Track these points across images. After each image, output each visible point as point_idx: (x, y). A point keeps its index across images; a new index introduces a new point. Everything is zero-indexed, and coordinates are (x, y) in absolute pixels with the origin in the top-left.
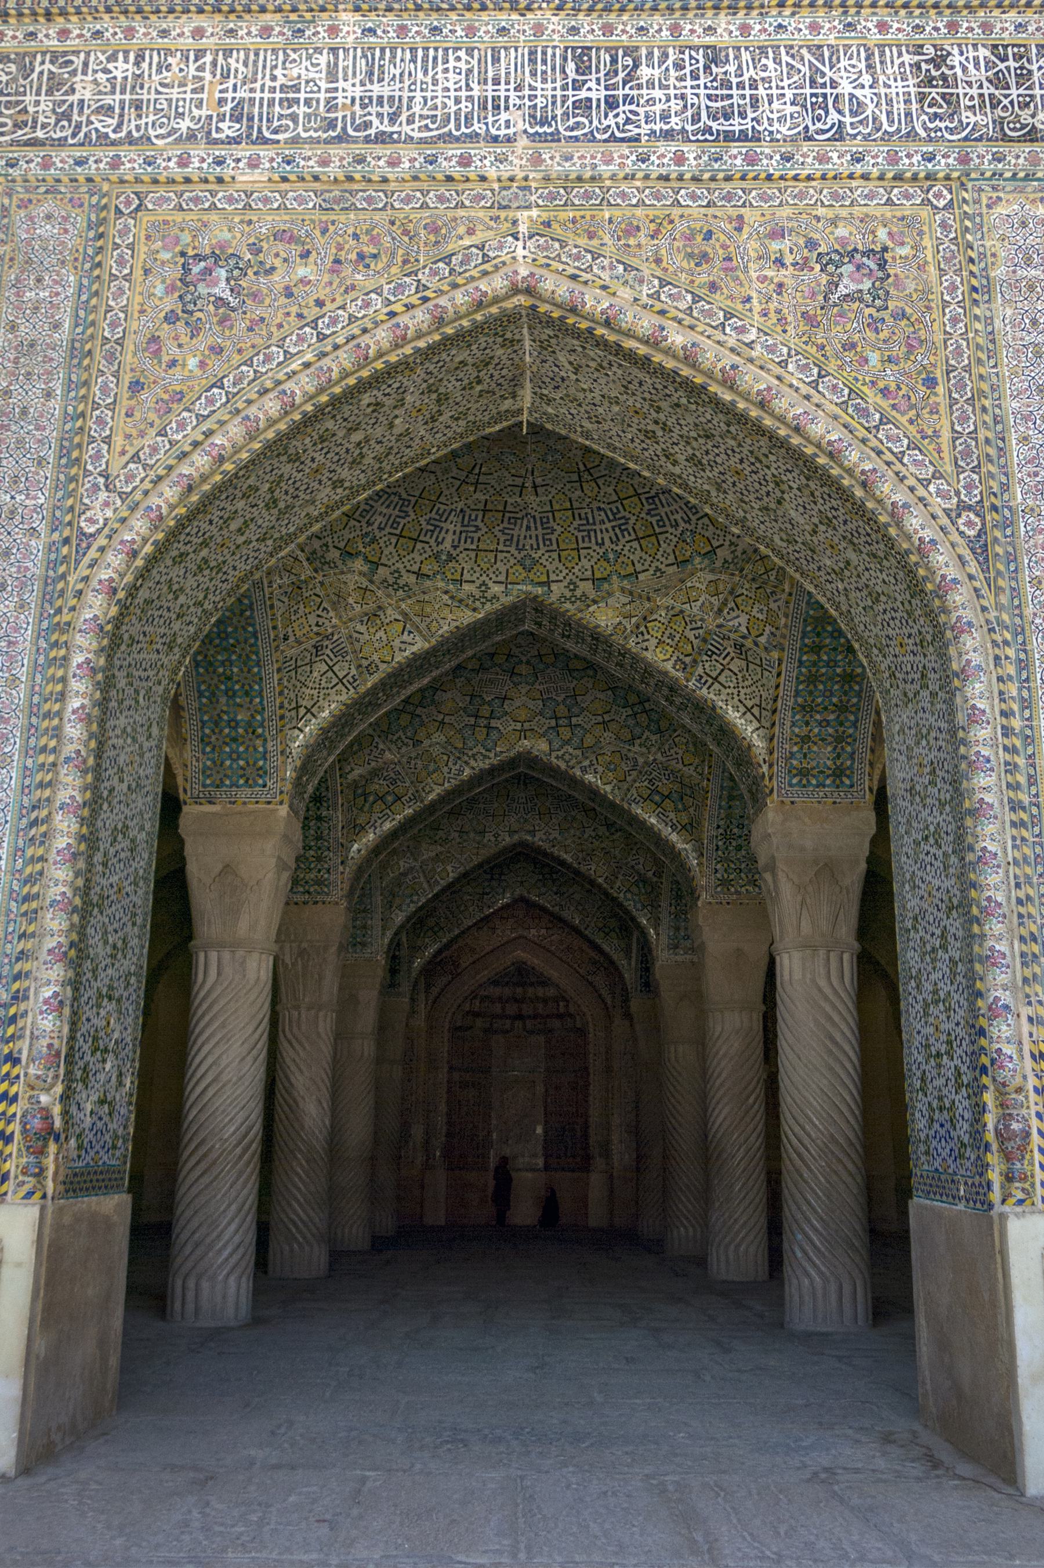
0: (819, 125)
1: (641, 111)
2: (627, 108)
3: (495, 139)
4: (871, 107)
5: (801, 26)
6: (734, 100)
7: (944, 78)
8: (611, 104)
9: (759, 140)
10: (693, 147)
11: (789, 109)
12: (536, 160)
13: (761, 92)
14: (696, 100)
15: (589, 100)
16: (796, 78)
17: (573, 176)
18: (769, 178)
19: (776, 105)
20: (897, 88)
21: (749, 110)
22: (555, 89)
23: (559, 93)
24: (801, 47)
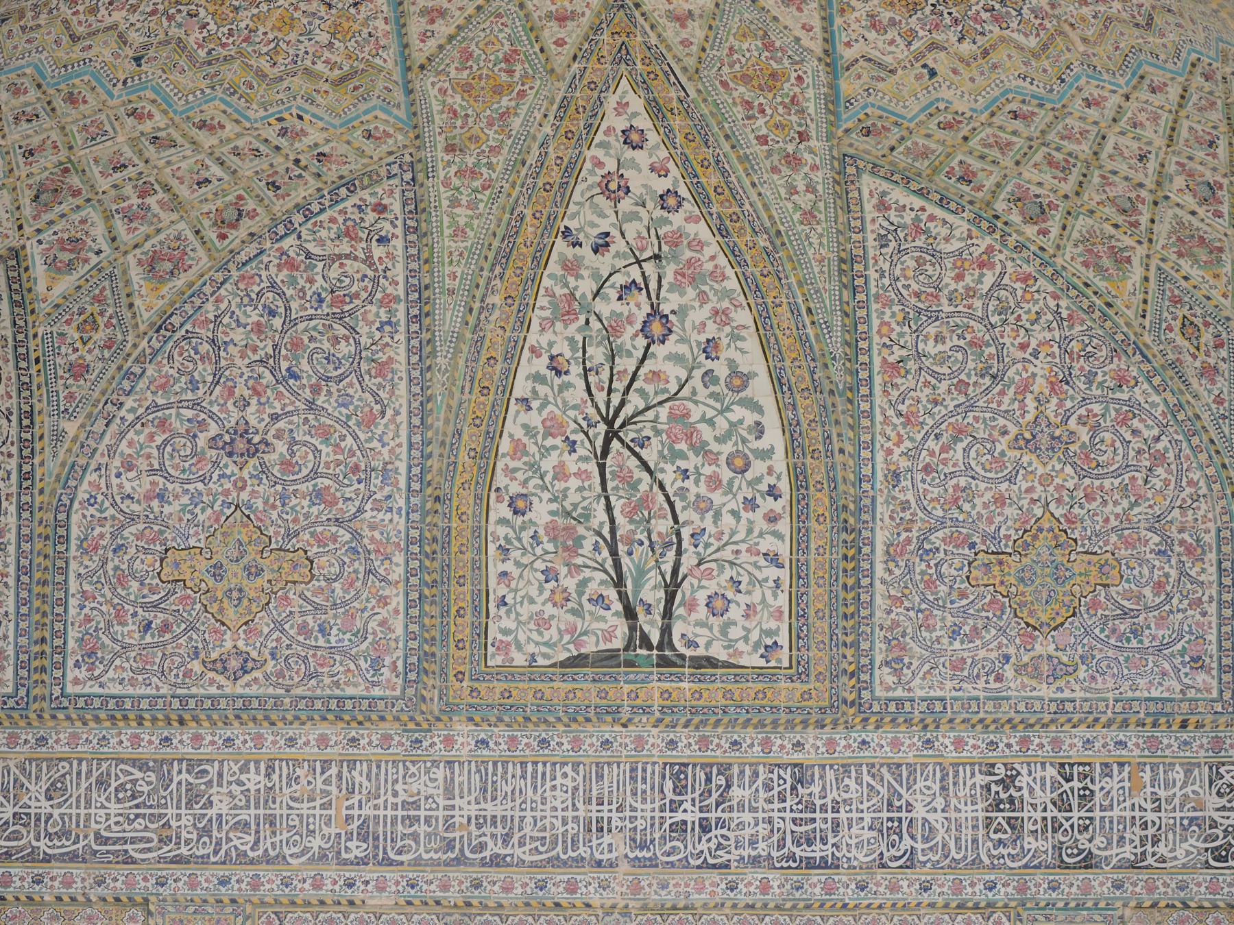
0: (893, 852)
1: (731, 835)
2: (719, 832)
3: (599, 864)
4: (942, 831)
5: (883, 742)
6: (819, 824)
7: (1011, 800)
8: (705, 828)
9: (837, 867)
10: (777, 874)
11: (868, 834)
12: (636, 888)
13: (843, 815)
14: (782, 825)
15: (685, 822)
16: (874, 801)
17: (668, 905)
18: (845, 906)
19: (854, 830)
20: (967, 812)
21: (830, 835)
22: (653, 810)
23: (657, 814)
24: (882, 765)
